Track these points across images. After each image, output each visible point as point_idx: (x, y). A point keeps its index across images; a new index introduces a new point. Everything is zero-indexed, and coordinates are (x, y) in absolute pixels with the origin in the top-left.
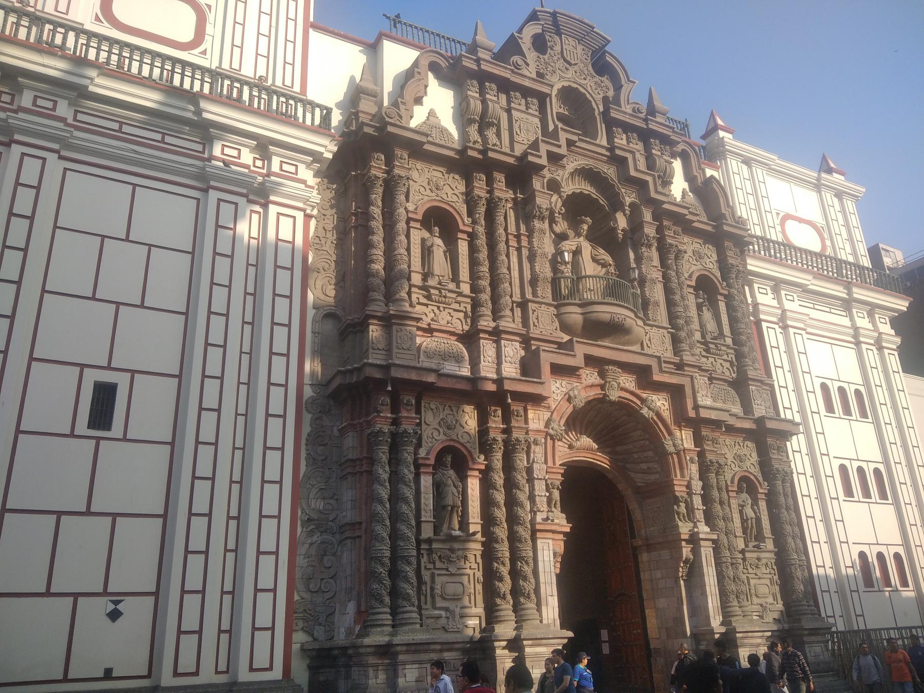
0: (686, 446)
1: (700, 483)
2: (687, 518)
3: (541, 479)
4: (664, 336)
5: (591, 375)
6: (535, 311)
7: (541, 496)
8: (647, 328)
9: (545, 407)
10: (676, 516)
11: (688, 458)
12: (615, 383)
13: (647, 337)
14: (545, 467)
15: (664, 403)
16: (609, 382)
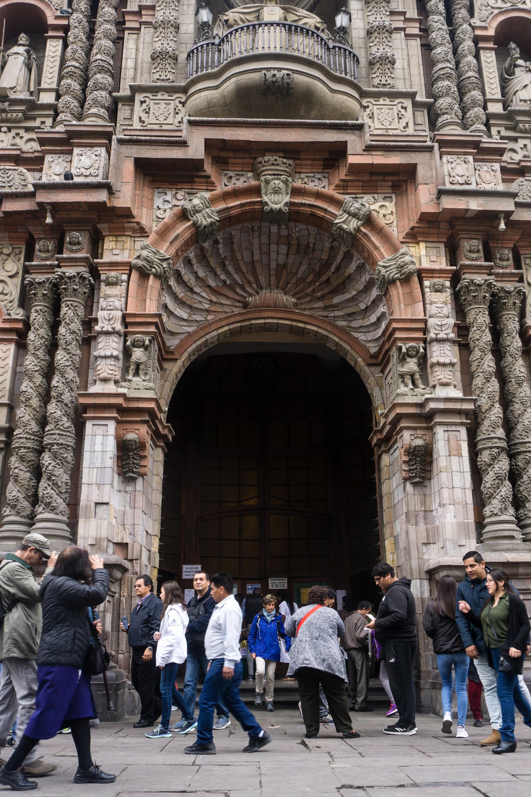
0: (426, 264)
1: (452, 321)
2: (419, 382)
3: (108, 333)
4: (402, 107)
5: (237, 177)
6: (145, 102)
7: (106, 357)
8: (364, 102)
9: (134, 230)
10: (400, 380)
11: (427, 283)
12: (277, 182)
13: (366, 114)
14: (119, 314)
15: (387, 204)
16: (267, 182)
